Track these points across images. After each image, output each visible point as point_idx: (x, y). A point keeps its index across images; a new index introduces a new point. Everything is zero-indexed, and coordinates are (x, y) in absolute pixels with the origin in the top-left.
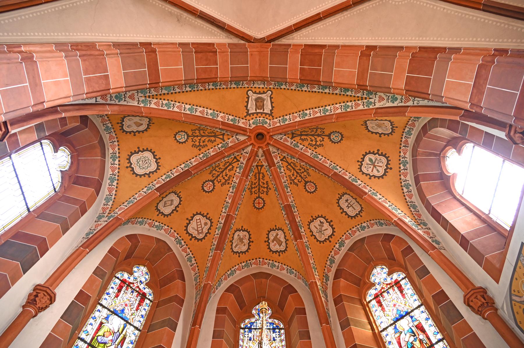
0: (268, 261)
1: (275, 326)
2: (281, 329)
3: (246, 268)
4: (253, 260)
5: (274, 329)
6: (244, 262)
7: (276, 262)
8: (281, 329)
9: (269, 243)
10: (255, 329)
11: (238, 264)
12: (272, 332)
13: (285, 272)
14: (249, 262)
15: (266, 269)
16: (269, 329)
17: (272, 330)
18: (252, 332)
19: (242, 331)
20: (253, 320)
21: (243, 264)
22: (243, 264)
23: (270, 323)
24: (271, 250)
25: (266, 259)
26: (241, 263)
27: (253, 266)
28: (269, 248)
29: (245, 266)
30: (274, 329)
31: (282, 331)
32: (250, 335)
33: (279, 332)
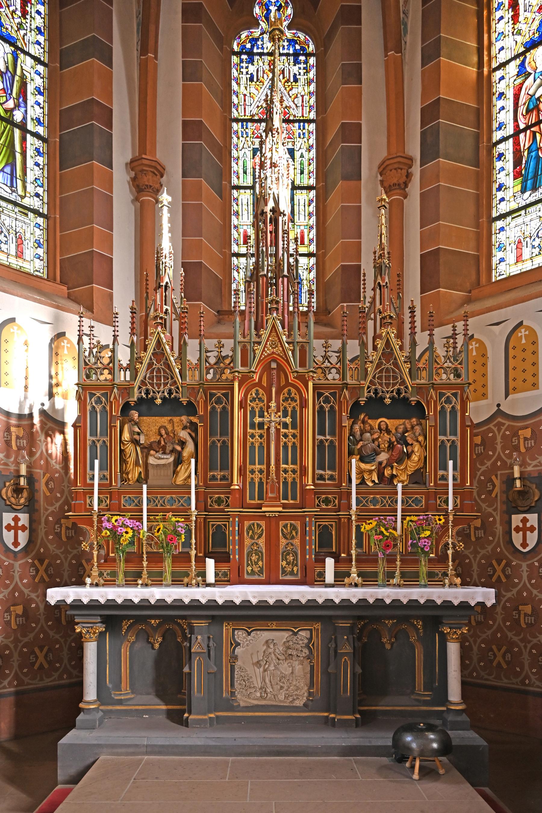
1: (298, 47)
5: (296, 55)
10: (261, 54)
16: (287, 55)
17: (292, 58)
19: (235, 59)
20: (257, 33)
23: (289, 41)
30: (296, 55)
31: (312, 61)
33: (306, 62)
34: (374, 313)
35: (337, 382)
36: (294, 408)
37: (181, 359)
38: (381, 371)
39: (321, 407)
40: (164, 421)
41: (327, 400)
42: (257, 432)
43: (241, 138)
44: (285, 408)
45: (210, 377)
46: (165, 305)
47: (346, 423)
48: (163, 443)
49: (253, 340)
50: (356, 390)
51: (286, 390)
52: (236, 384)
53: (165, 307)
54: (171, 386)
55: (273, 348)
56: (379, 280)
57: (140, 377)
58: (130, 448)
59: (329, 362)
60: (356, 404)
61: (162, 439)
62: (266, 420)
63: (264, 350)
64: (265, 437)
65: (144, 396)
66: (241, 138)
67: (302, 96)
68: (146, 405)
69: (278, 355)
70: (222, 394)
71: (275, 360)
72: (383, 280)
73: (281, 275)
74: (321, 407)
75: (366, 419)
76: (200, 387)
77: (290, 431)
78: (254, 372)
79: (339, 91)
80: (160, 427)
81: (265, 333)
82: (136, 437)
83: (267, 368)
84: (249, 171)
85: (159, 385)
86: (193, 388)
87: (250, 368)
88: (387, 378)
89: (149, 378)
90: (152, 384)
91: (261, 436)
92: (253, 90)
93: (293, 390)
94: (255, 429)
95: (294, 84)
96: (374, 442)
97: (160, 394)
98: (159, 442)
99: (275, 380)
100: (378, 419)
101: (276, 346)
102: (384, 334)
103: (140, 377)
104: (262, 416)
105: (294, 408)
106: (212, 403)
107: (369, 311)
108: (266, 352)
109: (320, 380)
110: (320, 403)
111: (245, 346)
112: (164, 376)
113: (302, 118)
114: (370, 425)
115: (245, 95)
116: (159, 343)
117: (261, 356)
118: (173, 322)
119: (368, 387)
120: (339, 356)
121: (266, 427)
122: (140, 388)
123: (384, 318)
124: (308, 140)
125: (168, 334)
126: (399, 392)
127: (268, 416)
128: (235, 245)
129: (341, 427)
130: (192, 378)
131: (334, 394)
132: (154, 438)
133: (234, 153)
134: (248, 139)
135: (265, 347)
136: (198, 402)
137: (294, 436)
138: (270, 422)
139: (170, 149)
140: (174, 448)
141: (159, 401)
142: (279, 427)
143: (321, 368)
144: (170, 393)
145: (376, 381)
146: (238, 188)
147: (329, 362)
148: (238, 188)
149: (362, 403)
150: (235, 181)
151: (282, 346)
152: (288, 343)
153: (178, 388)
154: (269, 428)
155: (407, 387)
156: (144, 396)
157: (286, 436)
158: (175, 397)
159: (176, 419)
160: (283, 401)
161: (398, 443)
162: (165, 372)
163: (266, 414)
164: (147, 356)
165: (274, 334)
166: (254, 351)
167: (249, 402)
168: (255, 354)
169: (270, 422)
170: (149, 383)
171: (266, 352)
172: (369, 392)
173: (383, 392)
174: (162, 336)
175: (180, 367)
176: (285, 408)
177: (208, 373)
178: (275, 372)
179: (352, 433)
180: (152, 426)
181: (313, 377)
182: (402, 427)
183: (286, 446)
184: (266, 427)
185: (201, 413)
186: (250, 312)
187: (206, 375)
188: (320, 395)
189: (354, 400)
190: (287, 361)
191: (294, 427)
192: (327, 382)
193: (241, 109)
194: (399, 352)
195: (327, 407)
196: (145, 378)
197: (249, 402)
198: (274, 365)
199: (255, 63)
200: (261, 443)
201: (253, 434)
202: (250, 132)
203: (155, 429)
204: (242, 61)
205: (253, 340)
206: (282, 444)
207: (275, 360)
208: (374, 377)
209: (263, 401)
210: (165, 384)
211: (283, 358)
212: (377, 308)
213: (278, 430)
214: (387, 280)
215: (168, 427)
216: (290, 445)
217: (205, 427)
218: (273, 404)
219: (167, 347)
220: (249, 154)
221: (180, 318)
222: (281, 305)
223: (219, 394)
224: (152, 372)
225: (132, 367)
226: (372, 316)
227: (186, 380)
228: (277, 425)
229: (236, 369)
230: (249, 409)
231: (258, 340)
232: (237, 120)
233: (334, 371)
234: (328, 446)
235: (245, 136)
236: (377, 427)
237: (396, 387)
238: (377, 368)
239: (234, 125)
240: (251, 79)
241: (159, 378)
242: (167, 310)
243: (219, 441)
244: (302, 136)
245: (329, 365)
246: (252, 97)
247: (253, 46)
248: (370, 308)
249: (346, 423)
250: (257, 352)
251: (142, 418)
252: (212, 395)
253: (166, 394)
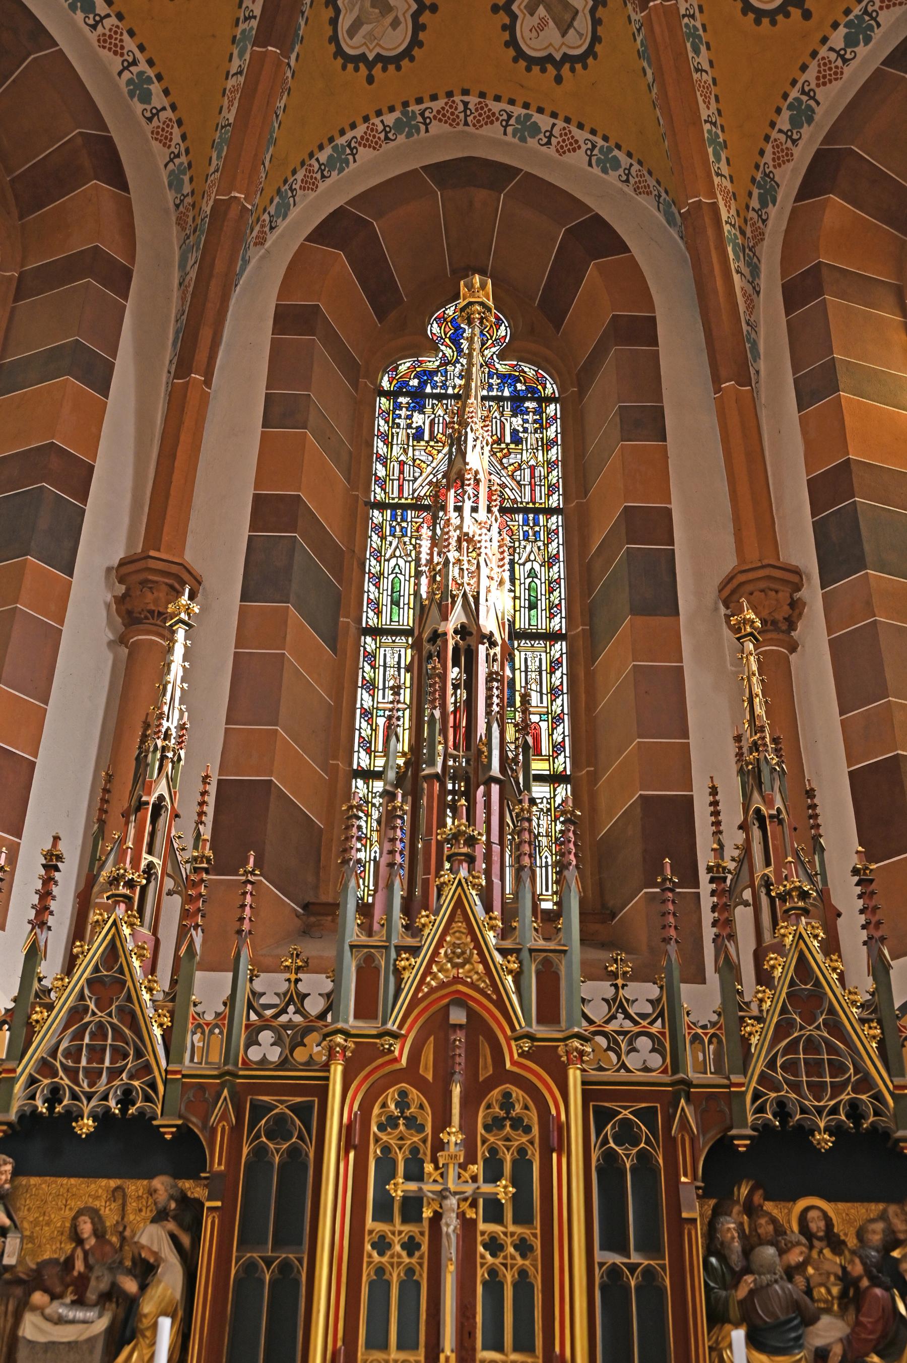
0: (503, 105)
1: (519, 386)
2: (550, 400)
3: (401, 138)
4: (434, 98)
6: (392, 109)
7: (540, 110)
8: (550, 400)
9: (514, 17)
10: (440, 397)
11: (366, 119)
12: (508, 412)
13: (578, 158)
14: (415, 108)
15: (492, 143)
16: (499, 399)
17: (508, 406)
18: (428, 410)
19: (384, 403)
20: (432, 363)
21: (390, 119)
22: (390, 119)
24: (520, 54)
25: (497, 99)
26: (379, 113)
27: (436, 128)
28: (512, 42)
29: (399, 126)
30: (517, 400)
32: (418, 419)
33: (539, 411)
34: (752, 885)
35: (654, 1076)
36: (522, 1151)
37: (173, 1000)
38: (792, 1048)
39: (610, 1157)
40: (95, 1191)
41: (626, 1134)
42: (398, 1230)
43: (390, 538)
44: (493, 1151)
45: (254, 1054)
46: (150, 852)
47: (694, 1210)
49: (395, 941)
50: (718, 1105)
51: (496, 1093)
52: (337, 1072)
53: (146, 858)
54: (131, 1077)
55: (455, 966)
56: (757, 802)
57: (39, 1049)
59: (628, 1016)
60: (722, 1149)
61: (79, 1253)
62: (428, 1188)
63: (428, 971)
64: (425, 1248)
65: (43, 1109)
66: (390, 538)
67: (532, 468)
69: (473, 986)
70: (293, 1108)
71: (460, 1001)
72: (769, 803)
73: (482, 778)
74: (610, 1157)
75: (757, 1198)
76: (223, 1085)
77: (508, 1230)
78: (395, 1036)
79: (614, 456)
80: (80, 1213)
81: (433, 924)
83: (438, 1025)
85: (93, 1076)
86: (201, 1087)
87: (384, 1023)
88: (814, 1067)
89: (67, 1054)
90: (72, 1073)
91: (411, 1246)
93: (517, 1093)
94: (389, 1219)
95: (512, 446)
96: (790, 1279)
97: (93, 1103)
99: (462, 1060)
100: (794, 1199)
101: (467, 961)
102: (788, 940)
103: (39, 1049)
104: (415, 1173)
105: (522, 1151)
106: (258, 1136)
107: (735, 881)
108: (435, 977)
109: (601, 1069)
110: (605, 1142)
111: (369, 958)
112: (114, 1049)
113: (531, 505)
114: (773, 1221)
116: (113, 952)
117: (418, 989)
118: (165, 897)
119: (757, 1096)
120: (659, 1000)
121: (427, 1213)
122: (32, 1081)
123: (783, 898)
124: (546, 545)
125: (145, 931)
126: (855, 1111)
127: (436, 1175)
128: (363, 754)
129: (679, 1224)
130: (200, 1055)
131: (647, 1116)
132: (54, 1249)
134: (407, 539)
135: (432, 961)
136: (213, 1130)
137: (523, 1247)
138: (442, 1195)
139: (219, 538)
140: (114, 1285)
141: (86, 1126)
142: (470, 1214)
143: (604, 1034)
144: (126, 1099)
145: (780, 1075)
147: (628, 1016)
149: (742, 1145)
151: (484, 961)
152: (504, 952)
153: (153, 1086)
154: (437, 1217)
155: (878, 1097)
156: (43, 1109)
157: (494, 1246)
158: (141, 1113)
160: (487, 1128)
161: (875, 1282)
163: (429, 1167)
165: (459, 925)
166: (398, 972)
167: (374, 1128)
168: (399, 981)
169: (442, 1195)
170: (65, 1068)
171: (435, 977)
172: (761, 1110)
173: (803, 1111)
174: (126, 931)
175: (166, 1021)
176: (493, 1151)
177: (252, 1041)
178: (460, 1037)
179: (714, 1246)
181: (582, 1053)
182: (879, 1226)
183: (494, 1286)
184: (427, 1213)
185: (219, 1167)
186: (391, 865)
187: (247, 1047)
188: (603, 1117)
189: (713, 1135)
190: (500, 1004)
191: (523, 1216)
192: (623, 1075)
194: (839, 991)
195: (628, 1157)
196: (54, 1053)
197: (374, 1128)
198: (458, 1016)
200: (410, 1271)
201: (382, 1237)
204: (399, 406)
205: (395, 941)
206: (481, 1274)
207: (460, 1001)
208: (772, 1064)
209: (421, 1128)
210: (114, 1073)
211: (488, 997)
212: (758, 874)
213: (468, 1226)
214: (779, 804)
215: (105, 1212)
216: (509, 1278)
217: (225, 1214)
218: (453, 1137)
219: (136, 963)
221: (186, 888)
222: (480, 850)
223: (281, 1109)
226: (747, 895)
227: (181, 1061)
228: (465, 1206)
229: (340, 1025)
230: (374, 1151)
231: (410, 941)
233: (644, 1043)
234: (638, 1288)
235: (398, 533)
236: (795, 1228)
237: (844, 1097)
238: (776, 1040)
241: (96, 1053)
242: (150, 866)
243: (268, 1262)
244: (532, 538)
245: (628, 1025)
246: (419, 467)
248: (737, 875)
249: (694, 1210)
250: (406, 975)
251: (24, 1181)
252: (259, 1110)
253: (112, 1103)
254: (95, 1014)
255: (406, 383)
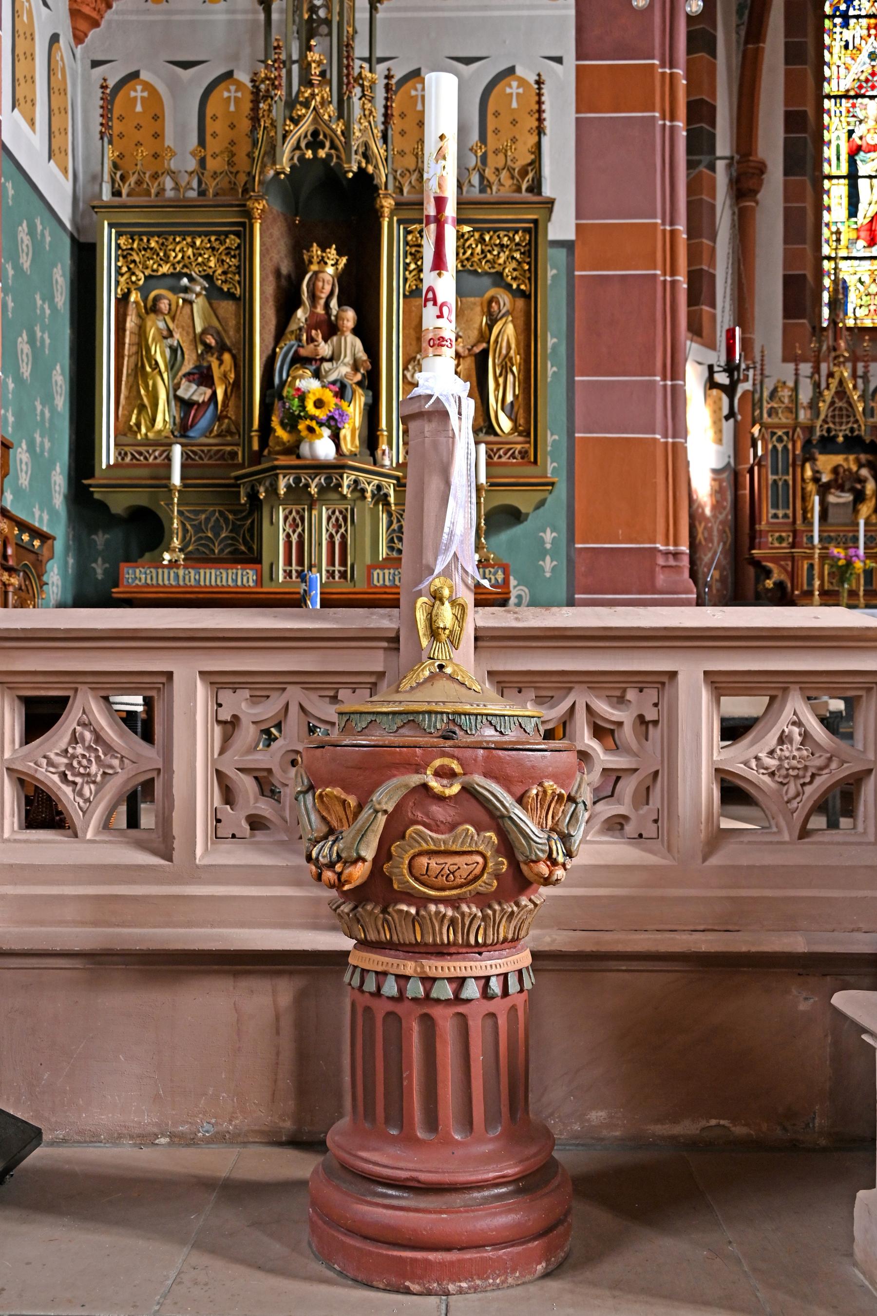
32: (847, 35)
48: (840, 481)
57: (822, 416)
58: (811, 487)
65: (826, 434)
68: (828, 444)
82: (818, 475)
84: (844, 157)
90: (834, 423)
92: (849, 60)
98: (836, 480)
103: (822, 416)
115: (838, 66)
122: (821, 426)
133: (827, 136)
141: (841, 439)
146: (830, 177)
148: (830, 177)
150: (826, 169)
156: (826, 434)
159: (852, 457)
162: (847, 410)
164: (828, 395)
180: (826, 463)
193: (834, 83)
199: (851, 27)
202: (843, 110)
203: (829, 467)
204: (835, 25)
210: (848, 423)
220: (844, 136)
224: (834, 410)
225: (813, 405)
232: (829, 97)
239: (826, 101)
240: (846, 47)
247: (848, 8)
254: (839, 404)
255: (838, 9)
